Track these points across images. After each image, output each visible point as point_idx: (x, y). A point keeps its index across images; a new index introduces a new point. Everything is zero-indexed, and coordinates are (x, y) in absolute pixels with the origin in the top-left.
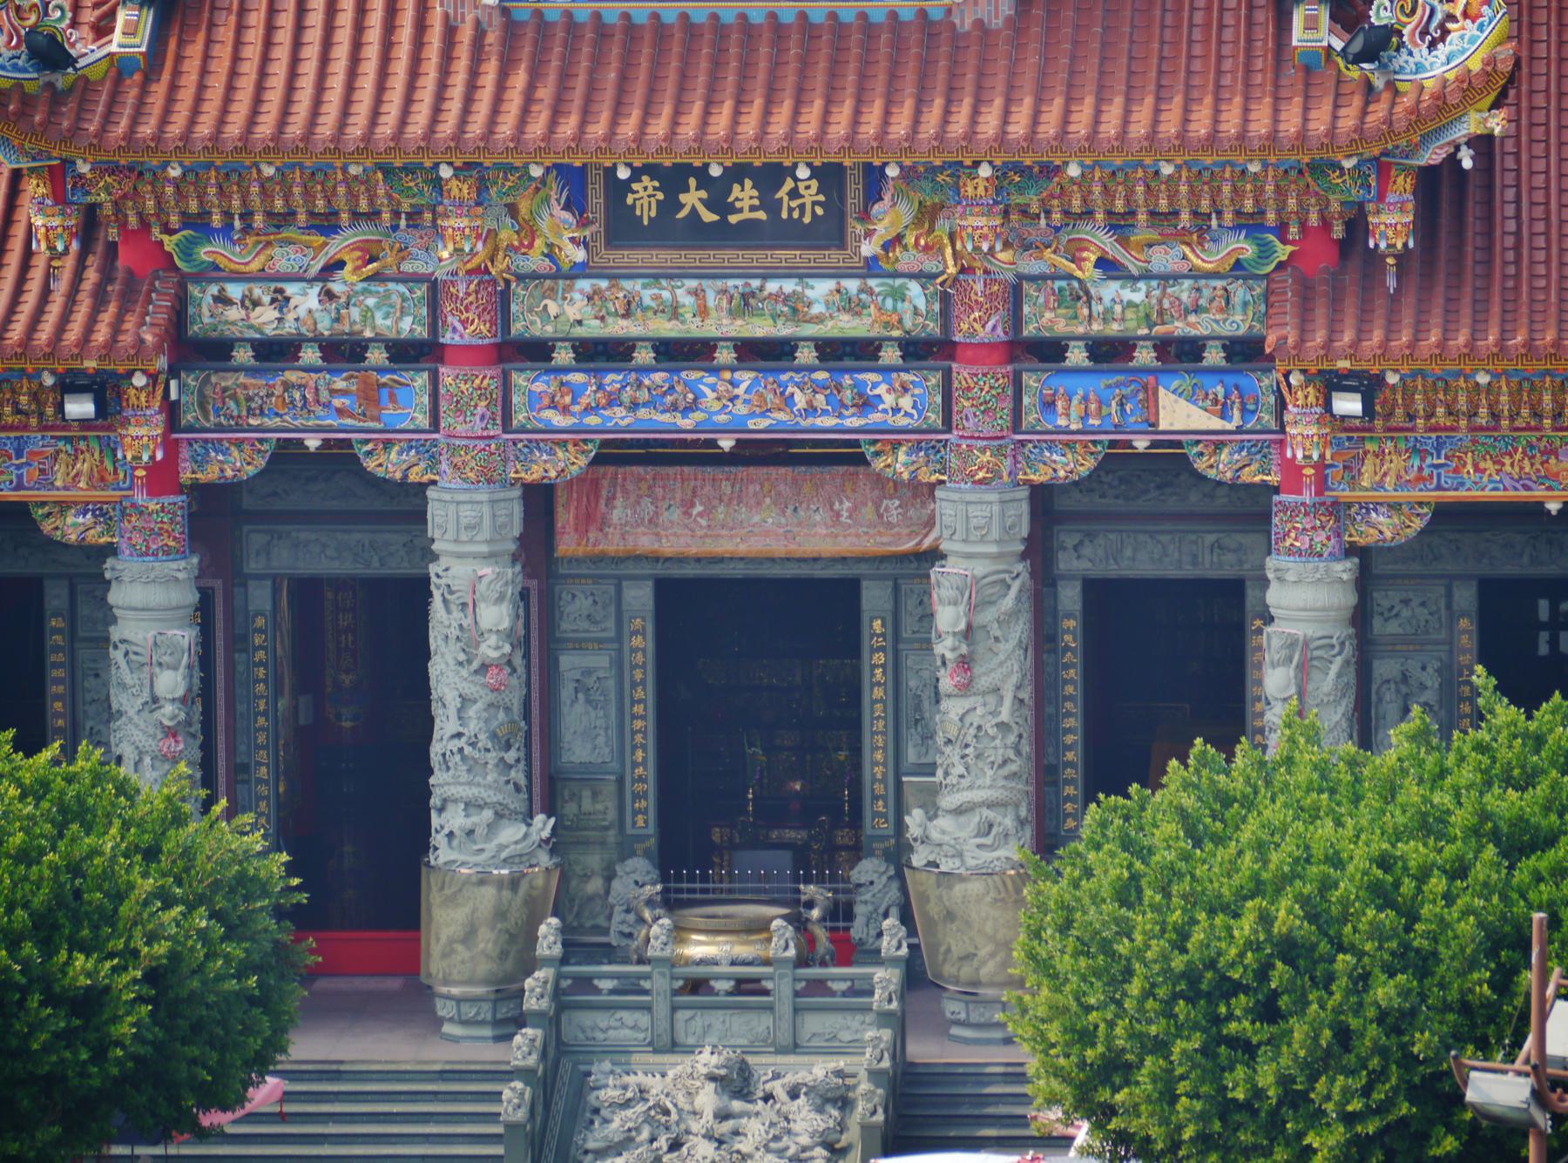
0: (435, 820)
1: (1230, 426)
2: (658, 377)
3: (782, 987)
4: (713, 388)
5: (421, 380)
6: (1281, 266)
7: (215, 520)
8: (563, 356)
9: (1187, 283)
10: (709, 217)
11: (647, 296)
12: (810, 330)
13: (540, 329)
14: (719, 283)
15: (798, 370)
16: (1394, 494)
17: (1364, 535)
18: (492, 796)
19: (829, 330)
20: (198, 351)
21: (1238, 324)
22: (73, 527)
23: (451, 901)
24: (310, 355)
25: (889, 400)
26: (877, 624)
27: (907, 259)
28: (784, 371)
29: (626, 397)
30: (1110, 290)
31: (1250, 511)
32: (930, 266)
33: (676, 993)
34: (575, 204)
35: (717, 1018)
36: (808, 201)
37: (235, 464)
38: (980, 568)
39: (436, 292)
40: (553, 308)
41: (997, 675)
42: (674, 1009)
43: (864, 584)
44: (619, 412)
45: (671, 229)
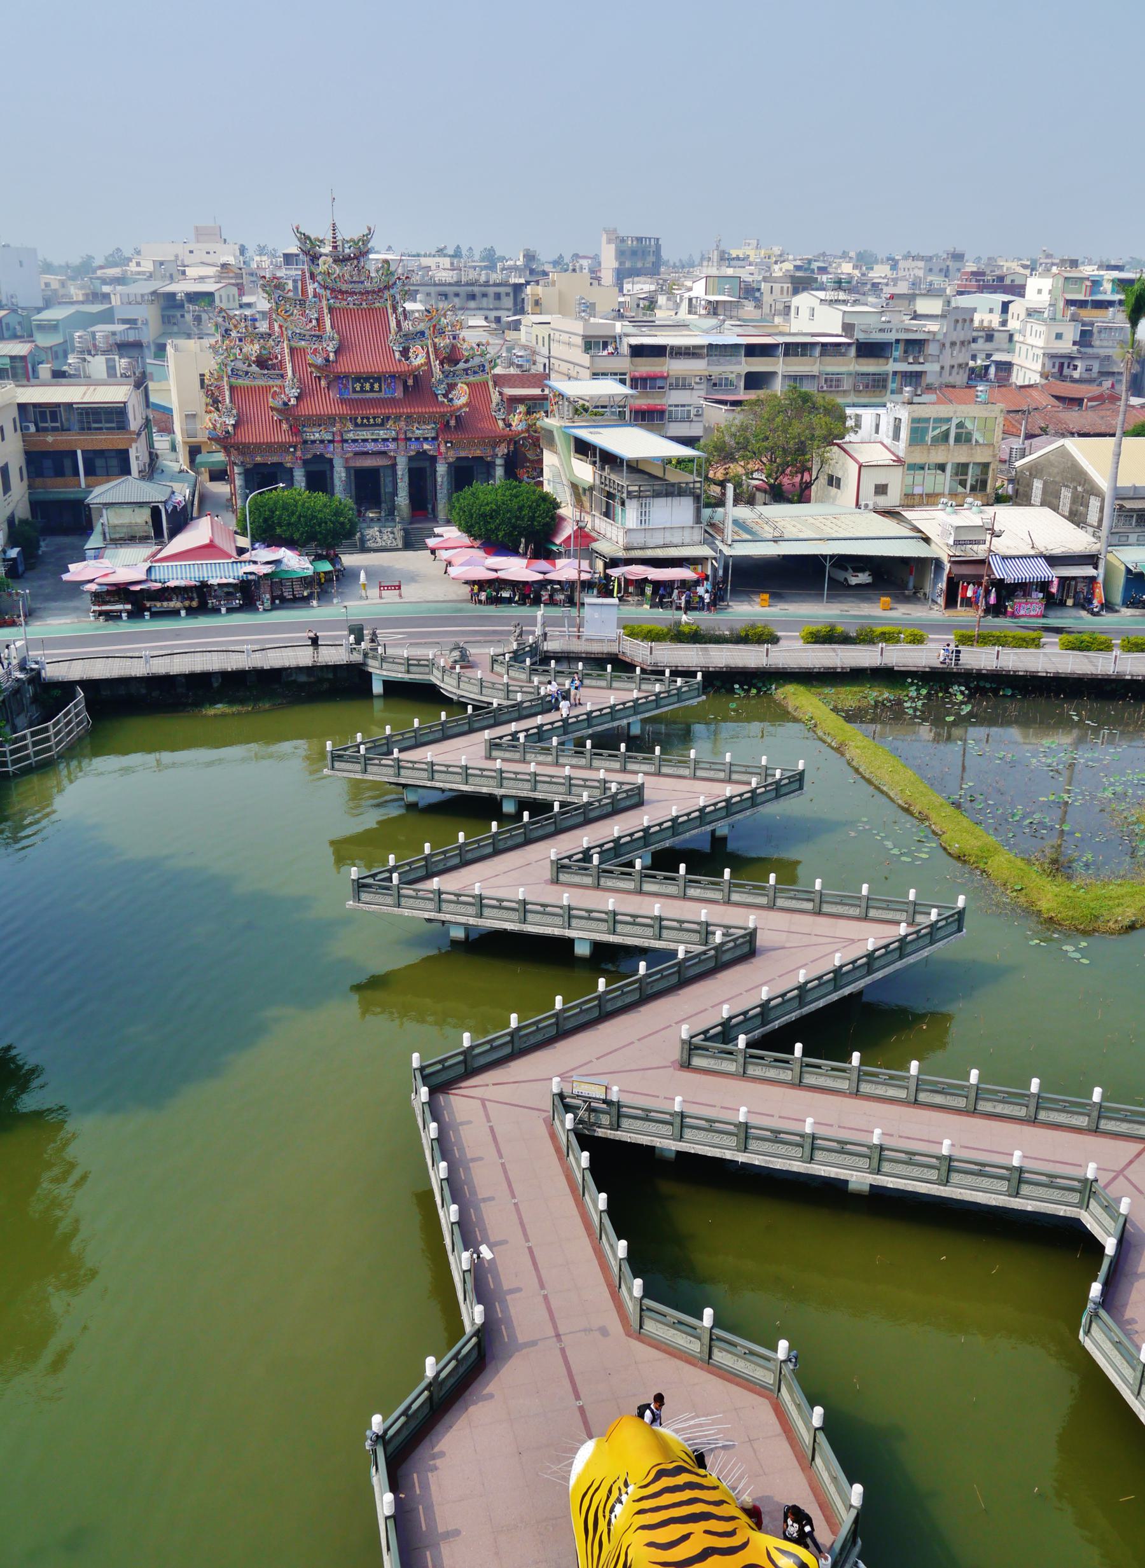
7: (306, 463)
16: (452, 456)
20: (305, 442)
21: (433, 435)
22: (289, 465)
31: (433, 460)
37: (309, 456)
39: (334, 434)
45: (362, 425)
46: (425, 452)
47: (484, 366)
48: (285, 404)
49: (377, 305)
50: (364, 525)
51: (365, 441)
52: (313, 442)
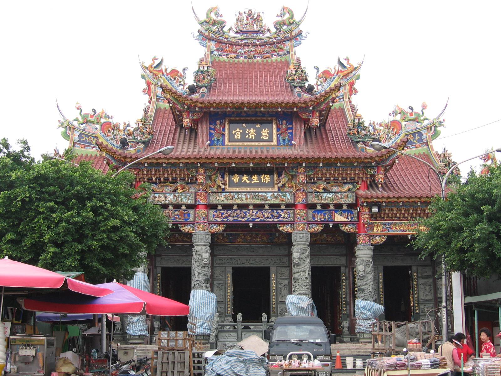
1: (348, 220)
2: (238, 211)
4: (249, 213)
5: (192, 212)
6: (358, 189)
8: (220, 207)
9: (339, 194)
10: (248, 182)
11: (236, 196)
13: (215, 202)
14: (250, 194)
15: (265, 210)
17: (375, 242)
21: (351, 200)
24: (171, 207)
25: (283, 215)
26: (273, 275)
27: (286, 189)
28: (262, 210)
30: (325, 195)
32: (290, 190)
33: (243, 329)
34: (223, 177)
36: (267, 179)
38: (302, 247)
40: (218, 198)
41: (305, 268)
43: (271, 267)
44: (231, 218)
45: (241, 184)
46: (337, 225)
47: (420, 134)
48: (124, 143)
49: (275, 58)
51: (246, 206)
52: (165, 207)
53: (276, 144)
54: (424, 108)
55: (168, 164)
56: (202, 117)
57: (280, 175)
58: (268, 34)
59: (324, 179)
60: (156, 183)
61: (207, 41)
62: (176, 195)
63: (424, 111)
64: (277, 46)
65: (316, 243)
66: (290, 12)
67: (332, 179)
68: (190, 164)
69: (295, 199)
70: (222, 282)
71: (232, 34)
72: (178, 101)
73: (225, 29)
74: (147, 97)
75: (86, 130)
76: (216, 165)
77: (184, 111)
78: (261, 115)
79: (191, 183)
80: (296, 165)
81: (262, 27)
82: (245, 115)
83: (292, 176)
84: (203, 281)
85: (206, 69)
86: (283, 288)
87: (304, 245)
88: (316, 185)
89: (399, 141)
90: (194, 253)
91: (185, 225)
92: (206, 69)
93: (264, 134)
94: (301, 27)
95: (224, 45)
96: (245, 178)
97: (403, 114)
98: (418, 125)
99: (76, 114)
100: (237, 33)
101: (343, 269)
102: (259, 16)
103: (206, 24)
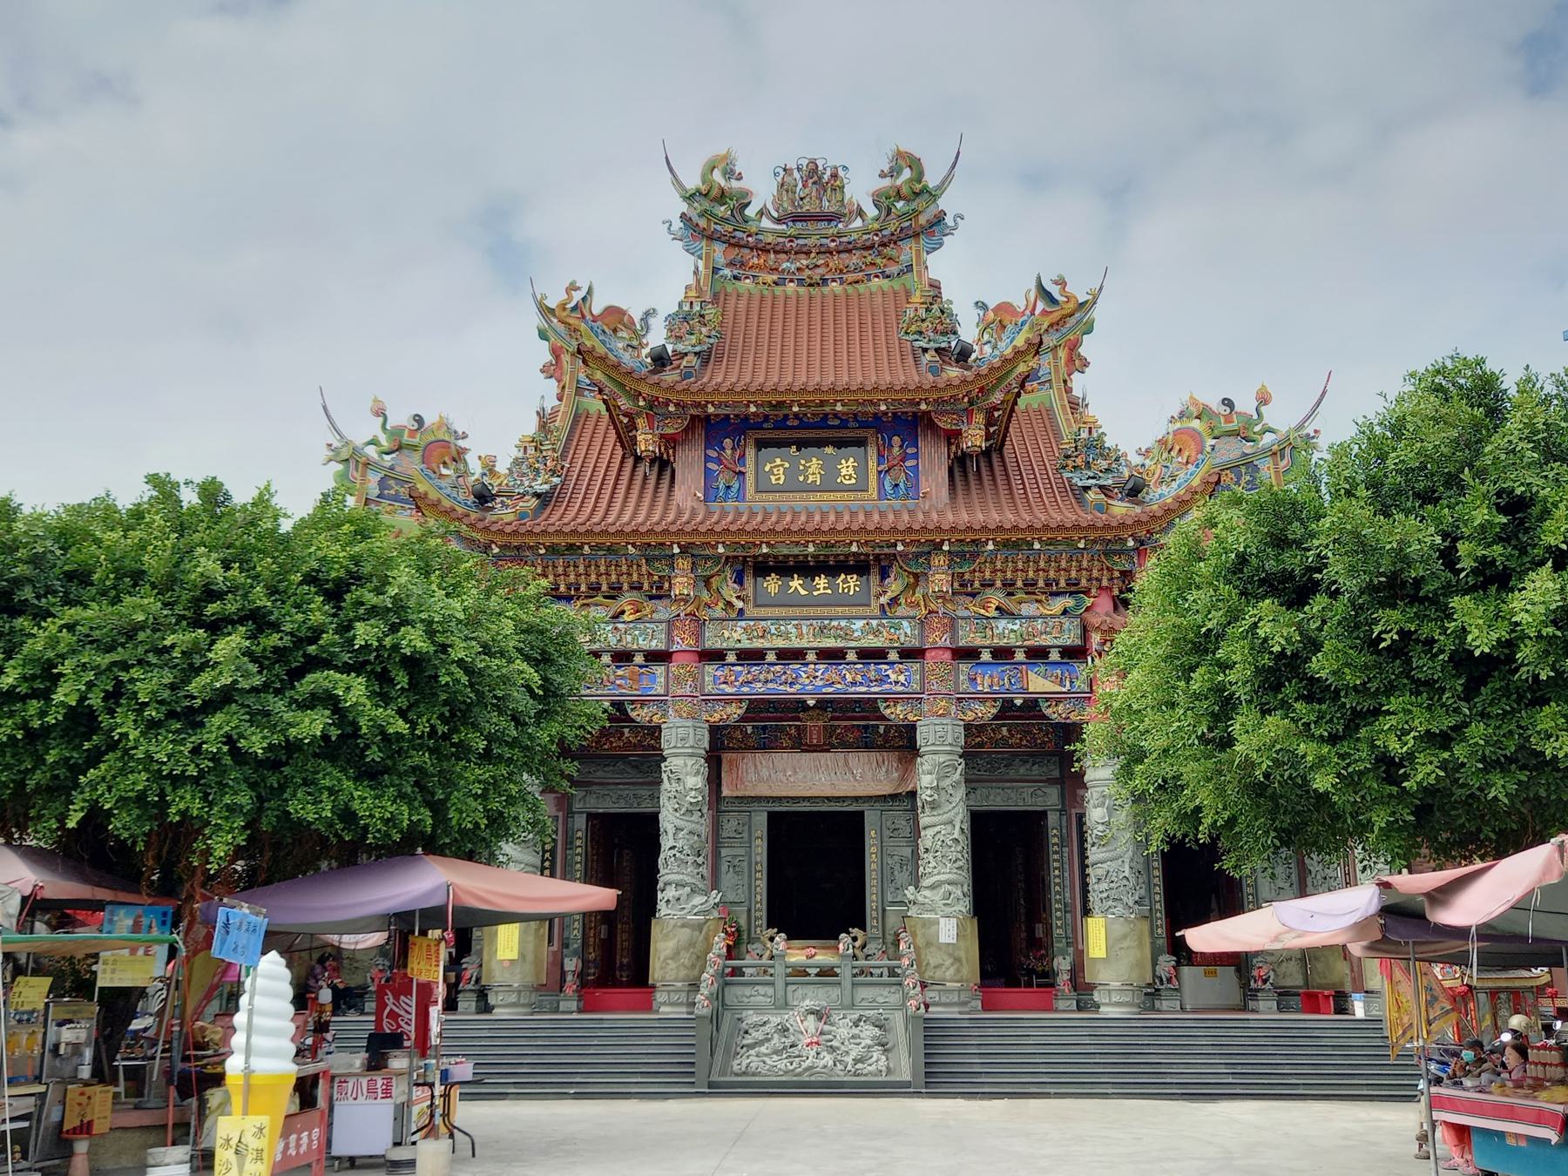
0: (660, 896)
2: (778, 668)
3: (846, 973)
5: (660, 670)
6: (1088, 609)
8: (731, 658)
12: (853, 644)
18: (689, 879)
19: (864, 643)
21: (1071, 638)
23: (666, 937)
25: (893, 677)
27: (901, 610)
29: (762, 677)
30: (1002, 624)
32: (912, 613)
33: (788, 975)
34: (739, 580)
35: (810, 990)
38: (942, 758)
40: (727, 634)
42: (787, 984)
46: (1032, 705)
50: (761, 995)
51: (797, 655)
53: (875, 496)
54: (1263, 399)
55: (596, 547)
56: (686, 430)
57: (884, 575)
58: (858, 223)
59: (999, 584)
60: (569, 599)
61: (704, 243)
62: (620, 626)
63: (1263, 409)
64: (880, 254)
65: (981, 753)
66: (915, 164)
67: (1019, 584)
68: (655, 550)
69: (922, 636)
70: (741, 851)
71: (766, 223)
72: (622, 386)
73: (750, 212)
74: (553, 382)
75: (398, 469)
76: (721, 550)
77: (639, 414)
78: (837, 422)
79: (659, 597)
80: (926, 549)
81: (843, 205)
82: (796, 423)
83: (916, 576)
84: (687, 850)
85: (697, 308)
86: (897, 867)
87: (949, 753)
88: (978, 599)
89: (1196, 482)
90: (664, 776)
91: (643, 703)
92: (697, 308)
93: (844, 472)
94: (943, 203)
95: (747, 251)
96: (796, 583)
97: (1205, 418)
98: (1248, 448)
99: (373, 428)
100: (778, 221)
101: (1052, 818)
102: (835, 176)
103: (702, 199)
